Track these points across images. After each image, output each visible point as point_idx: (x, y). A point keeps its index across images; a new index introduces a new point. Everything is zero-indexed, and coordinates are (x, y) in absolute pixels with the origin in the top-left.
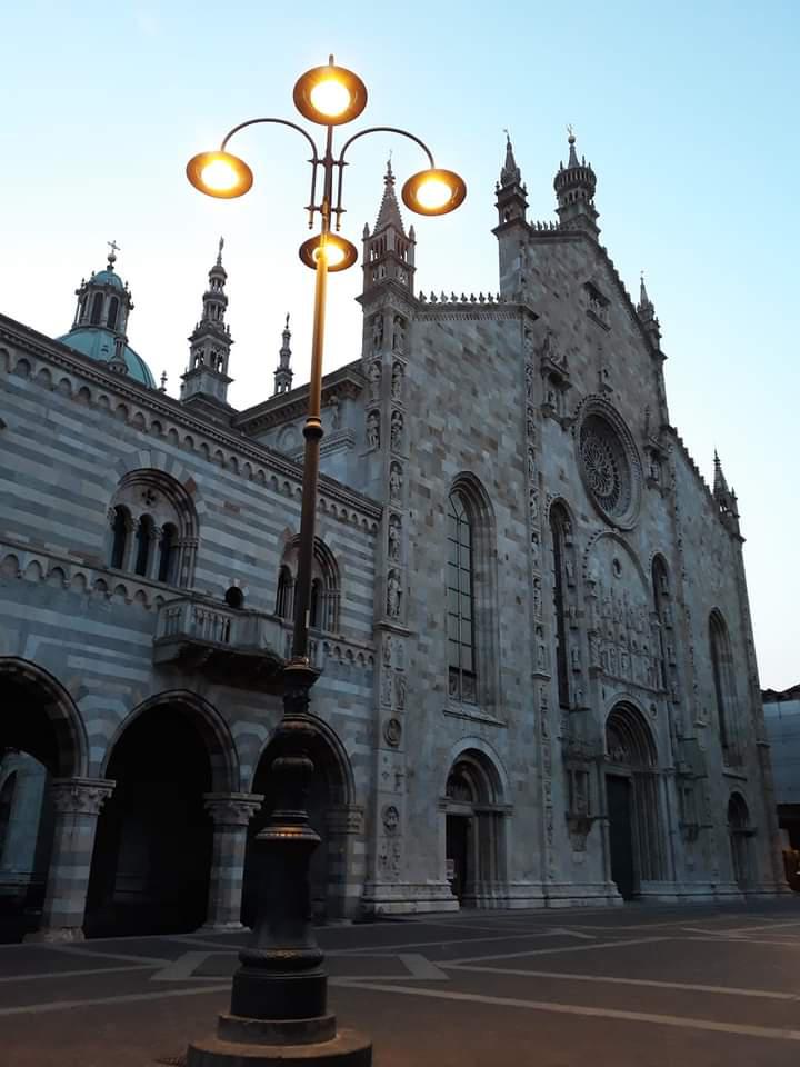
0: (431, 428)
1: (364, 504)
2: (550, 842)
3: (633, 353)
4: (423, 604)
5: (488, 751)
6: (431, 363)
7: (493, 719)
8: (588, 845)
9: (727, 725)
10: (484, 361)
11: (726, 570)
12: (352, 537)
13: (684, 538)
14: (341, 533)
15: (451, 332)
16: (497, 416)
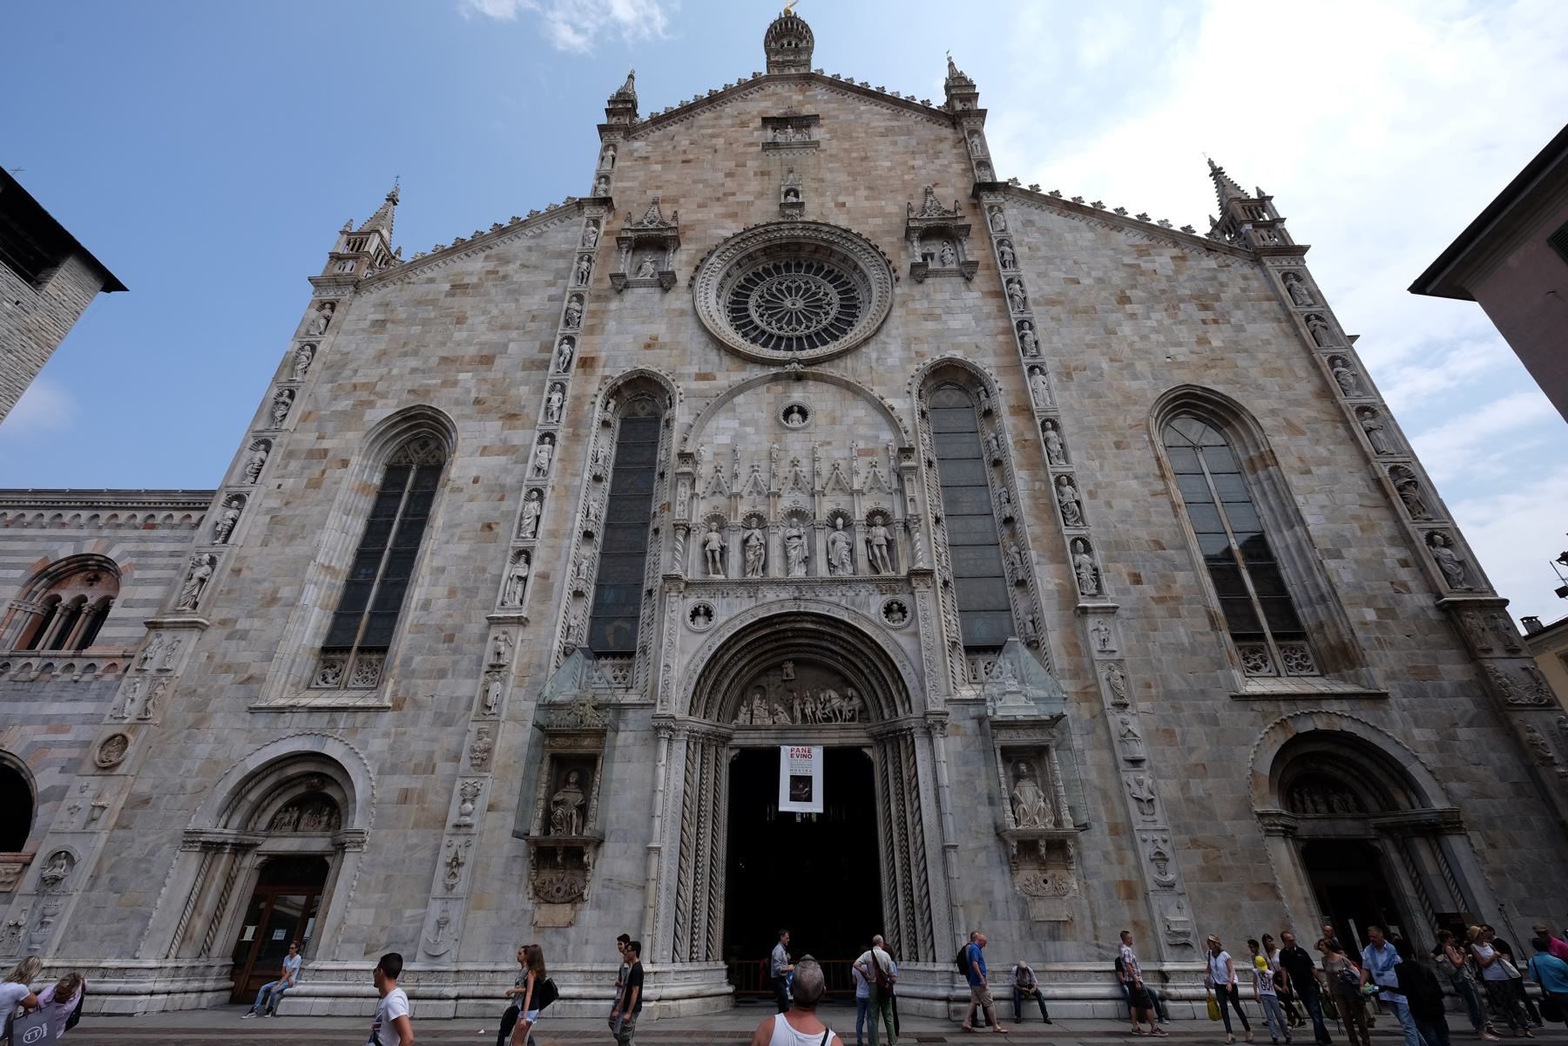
0: (355, 386)
1: (184, 499)
2: (449, 888)
3: (895, 143)
4: (258, 582)
5: (333, 750)
6: (380, 325)
7: (371, 701)
8: (593, 889)
9: (1294, 590)
10: (489, 284)
11: (1237, 316)
12: (163, 539)
13: (1036, 313)
14: (142, 540)
15: (431, 281)
16: (504, 327)
